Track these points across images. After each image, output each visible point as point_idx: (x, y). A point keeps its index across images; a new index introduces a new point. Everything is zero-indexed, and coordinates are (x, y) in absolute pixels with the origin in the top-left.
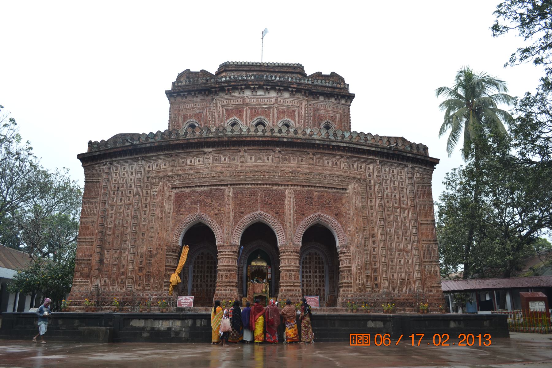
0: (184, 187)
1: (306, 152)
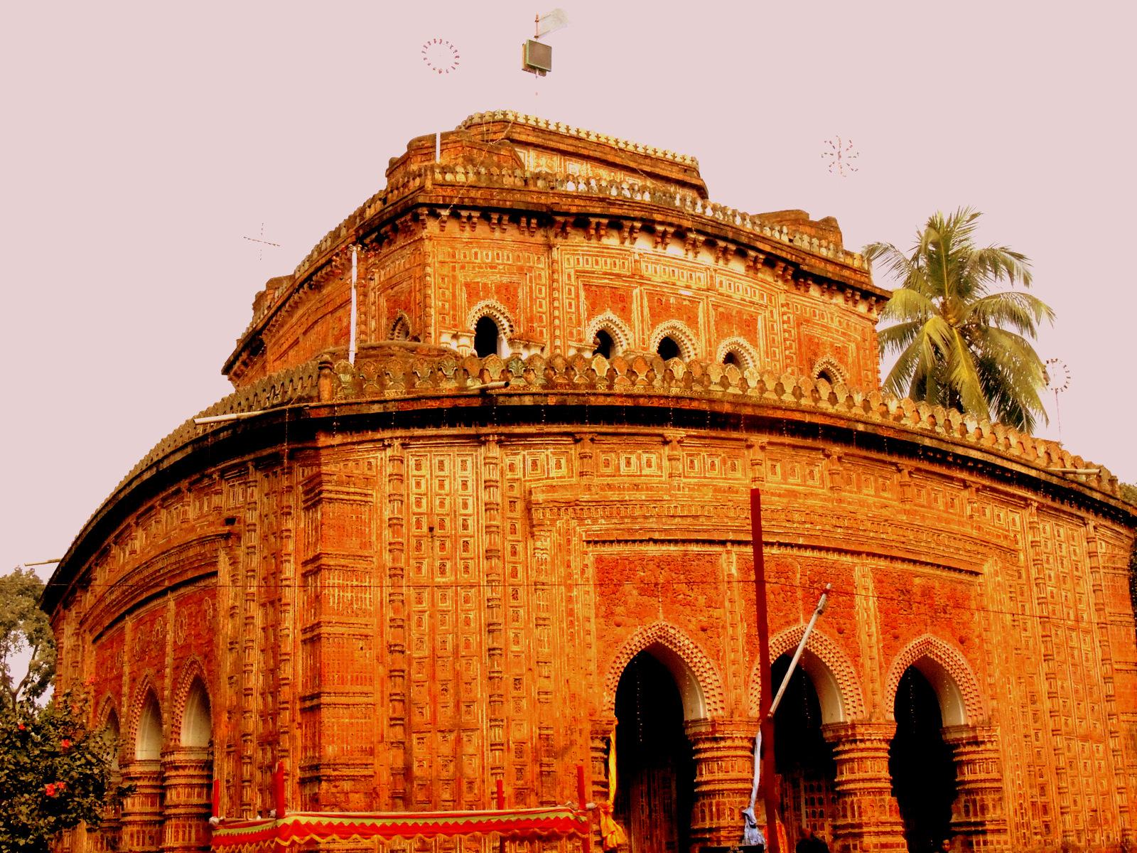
0: (619, 542)
1: (895, 464)
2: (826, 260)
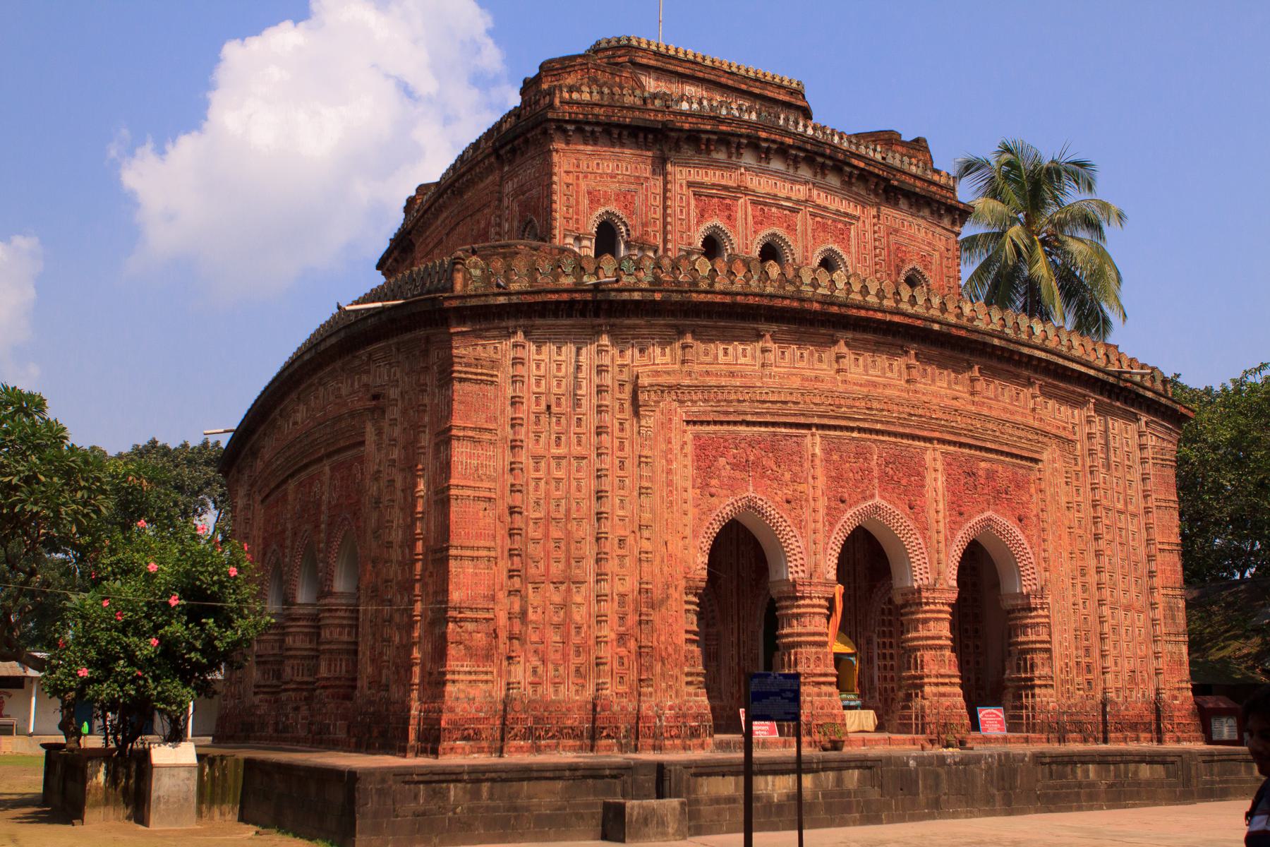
0: (715, 423)
2: (916, 177)
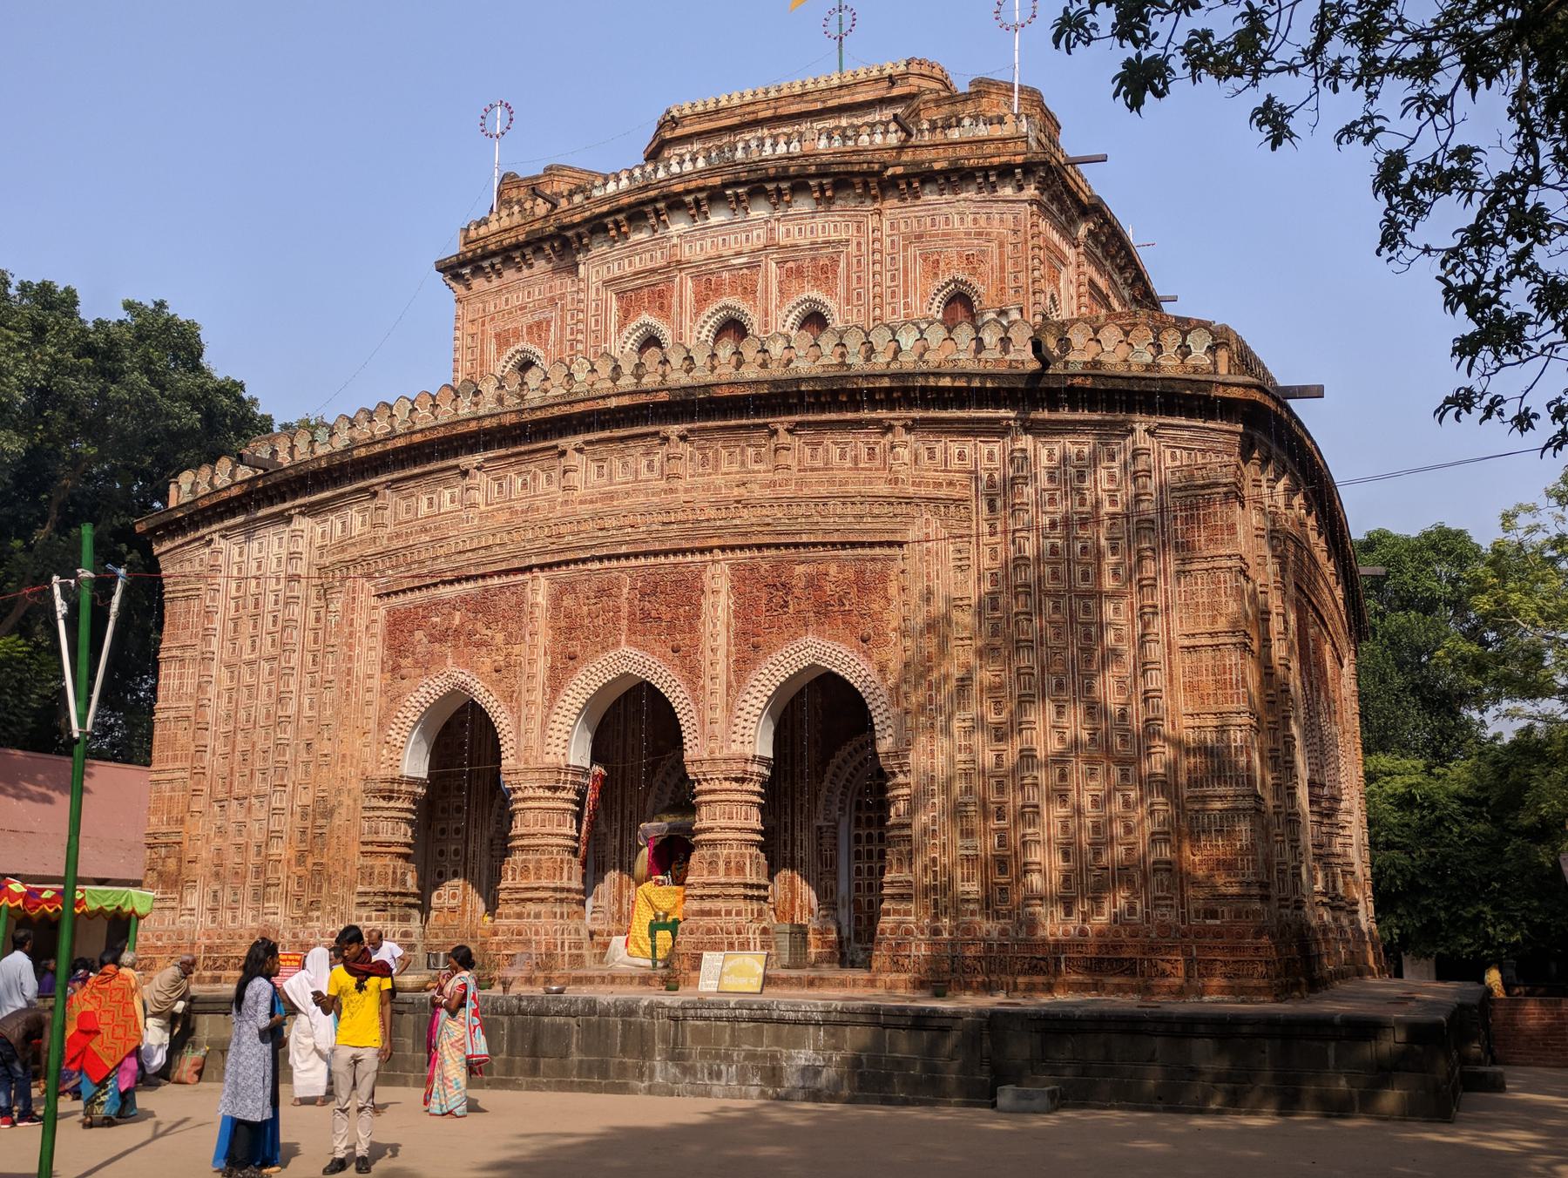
0: (412, 590)
1: (766, 425)
